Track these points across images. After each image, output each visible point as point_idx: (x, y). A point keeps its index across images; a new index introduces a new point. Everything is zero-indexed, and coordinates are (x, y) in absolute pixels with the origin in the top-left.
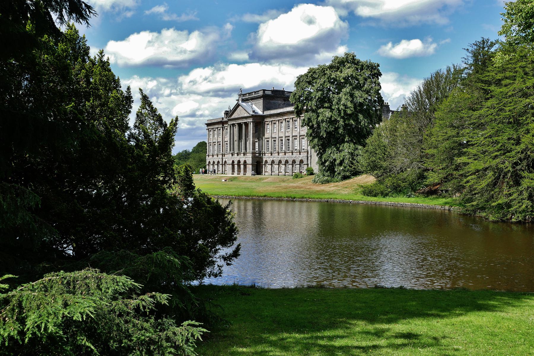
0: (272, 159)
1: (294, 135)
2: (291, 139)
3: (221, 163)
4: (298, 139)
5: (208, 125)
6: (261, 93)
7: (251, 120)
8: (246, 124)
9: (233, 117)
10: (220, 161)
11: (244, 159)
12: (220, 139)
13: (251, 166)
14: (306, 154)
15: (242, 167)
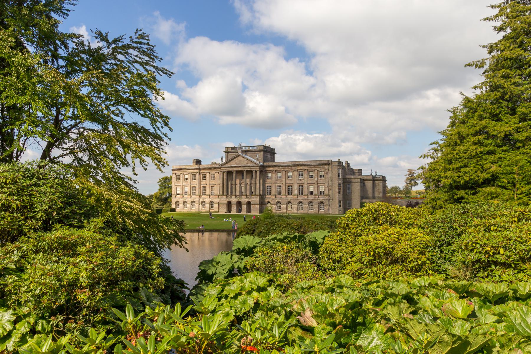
0: (277, 200)
1: (309, 182)
2: (305, 186)
3: (197, 202)
4: (316, 186)
5: (173, 170)
6: (262, 148)
7: (258, 168)
8: (250, 172)
9: (226, 166)
10: (197, 202)
11: (247, 200)
12: (196, 183)
13: (258, 206)
14: (327, 198)
15: (244, 206)
